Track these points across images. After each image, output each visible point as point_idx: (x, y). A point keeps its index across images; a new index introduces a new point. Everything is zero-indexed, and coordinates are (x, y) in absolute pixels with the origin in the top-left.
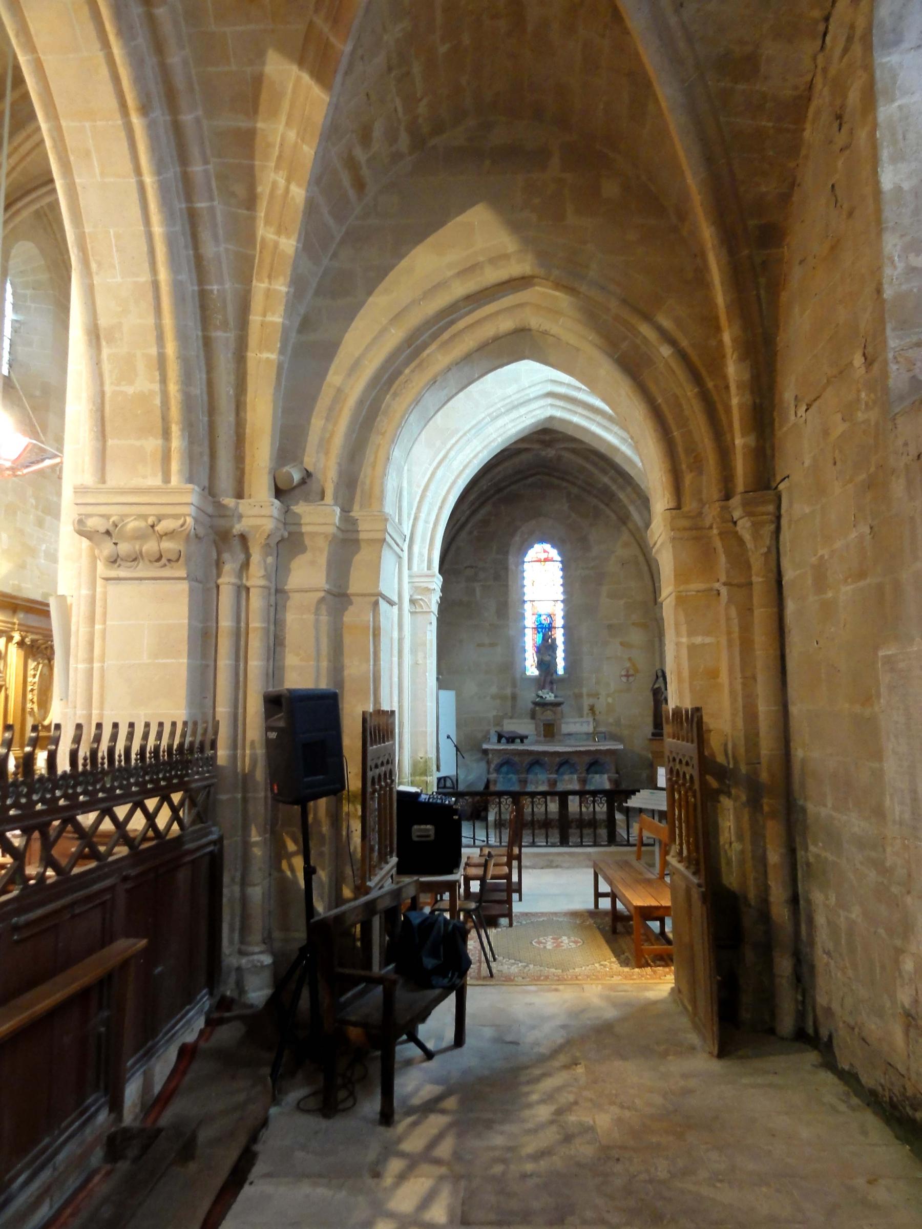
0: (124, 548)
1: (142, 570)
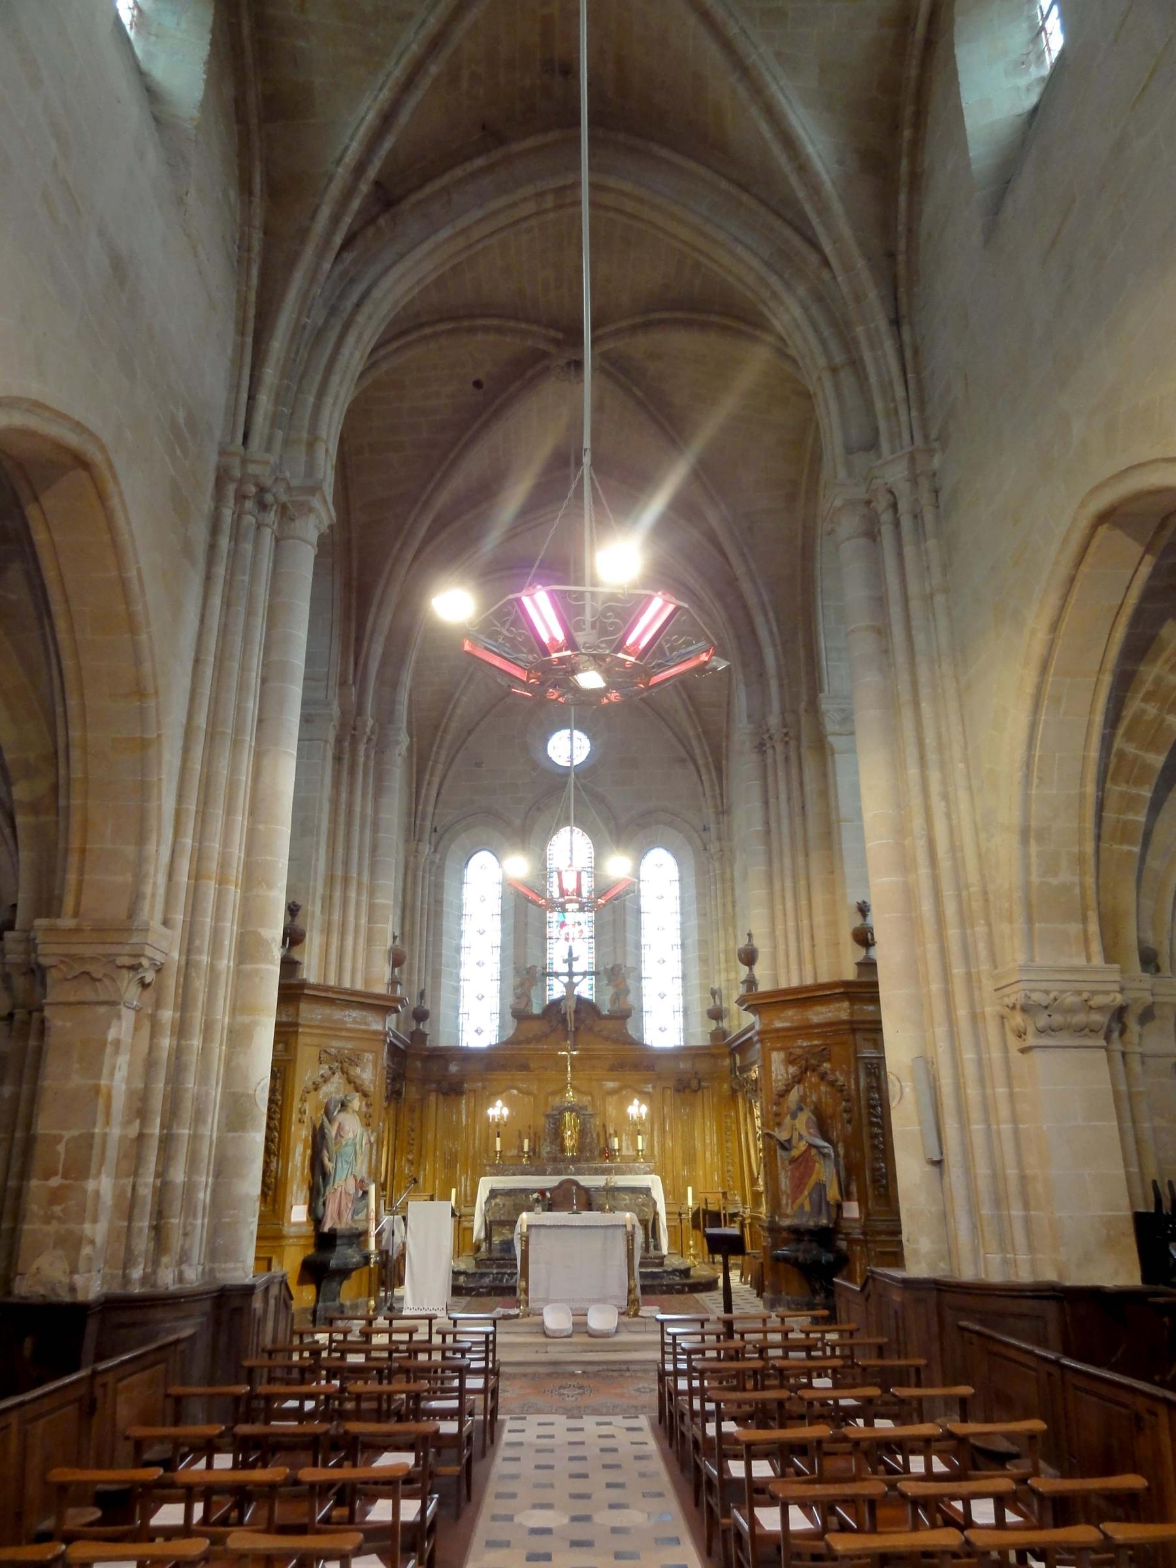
0: (1058, 1019)
1: (1065, 1039)
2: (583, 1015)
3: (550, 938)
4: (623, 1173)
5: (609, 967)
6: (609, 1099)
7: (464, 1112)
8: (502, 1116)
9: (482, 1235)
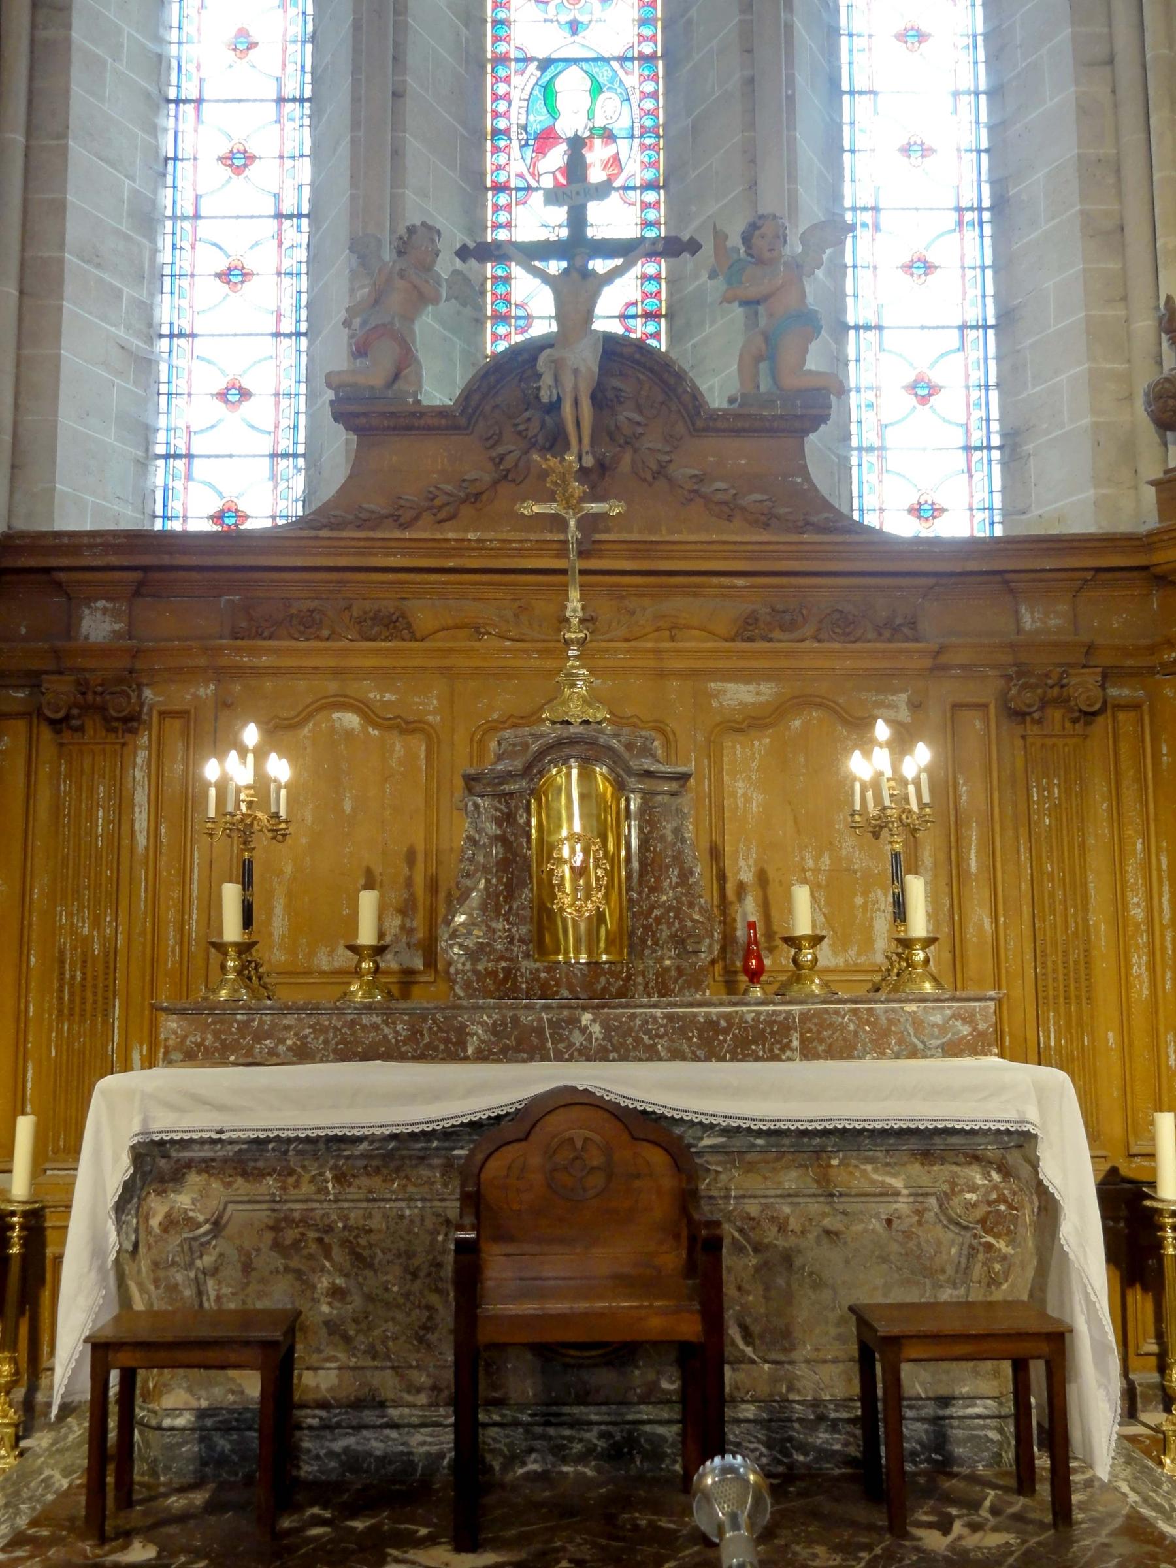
2: (626, 414)
3: (499, 188)
4: (843, 1050)
5: (735, 240)
6: (735, 750)
7: (141, 796)
8: (262, 783)
9: (84, 1392)
